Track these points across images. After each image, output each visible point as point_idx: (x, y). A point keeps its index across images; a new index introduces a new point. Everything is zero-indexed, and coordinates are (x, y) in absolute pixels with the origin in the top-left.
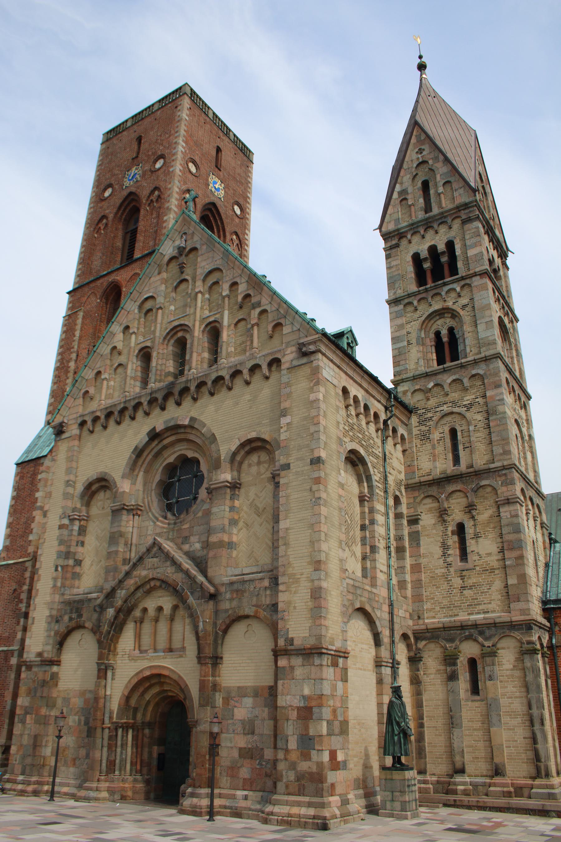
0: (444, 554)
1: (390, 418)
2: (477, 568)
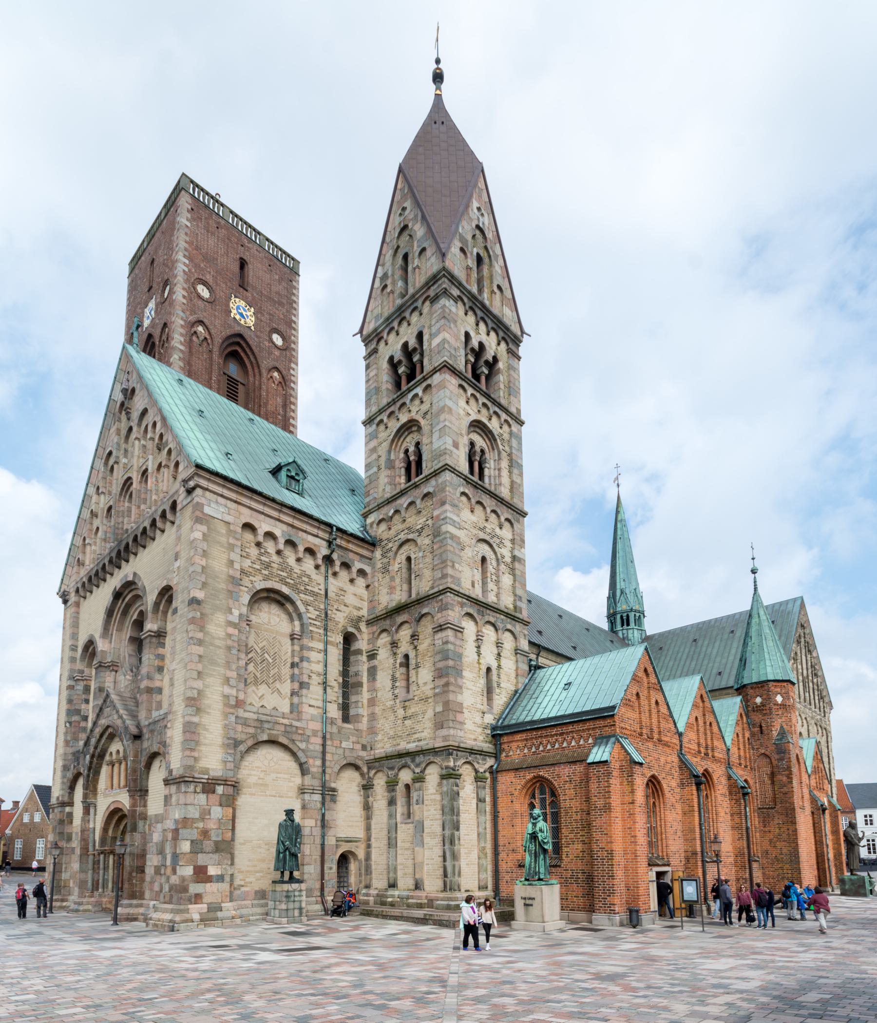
0: (393, 687)
1: (331, 553)
2: (416, 698)
